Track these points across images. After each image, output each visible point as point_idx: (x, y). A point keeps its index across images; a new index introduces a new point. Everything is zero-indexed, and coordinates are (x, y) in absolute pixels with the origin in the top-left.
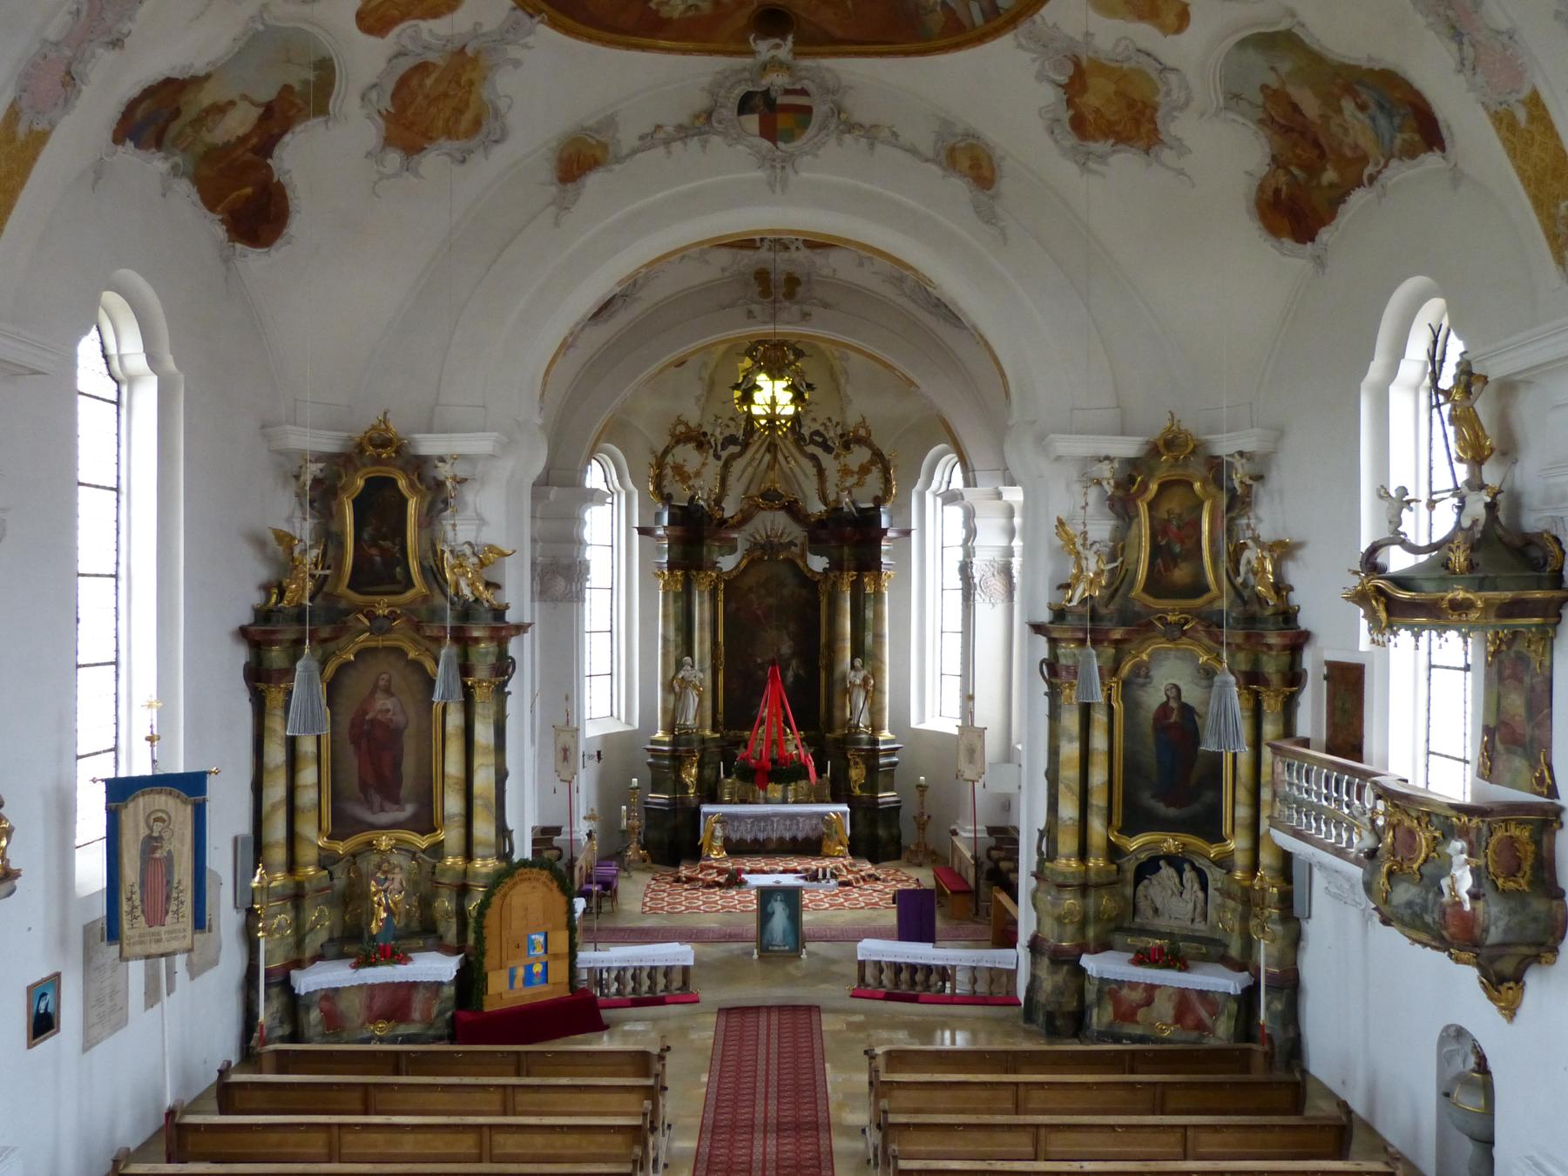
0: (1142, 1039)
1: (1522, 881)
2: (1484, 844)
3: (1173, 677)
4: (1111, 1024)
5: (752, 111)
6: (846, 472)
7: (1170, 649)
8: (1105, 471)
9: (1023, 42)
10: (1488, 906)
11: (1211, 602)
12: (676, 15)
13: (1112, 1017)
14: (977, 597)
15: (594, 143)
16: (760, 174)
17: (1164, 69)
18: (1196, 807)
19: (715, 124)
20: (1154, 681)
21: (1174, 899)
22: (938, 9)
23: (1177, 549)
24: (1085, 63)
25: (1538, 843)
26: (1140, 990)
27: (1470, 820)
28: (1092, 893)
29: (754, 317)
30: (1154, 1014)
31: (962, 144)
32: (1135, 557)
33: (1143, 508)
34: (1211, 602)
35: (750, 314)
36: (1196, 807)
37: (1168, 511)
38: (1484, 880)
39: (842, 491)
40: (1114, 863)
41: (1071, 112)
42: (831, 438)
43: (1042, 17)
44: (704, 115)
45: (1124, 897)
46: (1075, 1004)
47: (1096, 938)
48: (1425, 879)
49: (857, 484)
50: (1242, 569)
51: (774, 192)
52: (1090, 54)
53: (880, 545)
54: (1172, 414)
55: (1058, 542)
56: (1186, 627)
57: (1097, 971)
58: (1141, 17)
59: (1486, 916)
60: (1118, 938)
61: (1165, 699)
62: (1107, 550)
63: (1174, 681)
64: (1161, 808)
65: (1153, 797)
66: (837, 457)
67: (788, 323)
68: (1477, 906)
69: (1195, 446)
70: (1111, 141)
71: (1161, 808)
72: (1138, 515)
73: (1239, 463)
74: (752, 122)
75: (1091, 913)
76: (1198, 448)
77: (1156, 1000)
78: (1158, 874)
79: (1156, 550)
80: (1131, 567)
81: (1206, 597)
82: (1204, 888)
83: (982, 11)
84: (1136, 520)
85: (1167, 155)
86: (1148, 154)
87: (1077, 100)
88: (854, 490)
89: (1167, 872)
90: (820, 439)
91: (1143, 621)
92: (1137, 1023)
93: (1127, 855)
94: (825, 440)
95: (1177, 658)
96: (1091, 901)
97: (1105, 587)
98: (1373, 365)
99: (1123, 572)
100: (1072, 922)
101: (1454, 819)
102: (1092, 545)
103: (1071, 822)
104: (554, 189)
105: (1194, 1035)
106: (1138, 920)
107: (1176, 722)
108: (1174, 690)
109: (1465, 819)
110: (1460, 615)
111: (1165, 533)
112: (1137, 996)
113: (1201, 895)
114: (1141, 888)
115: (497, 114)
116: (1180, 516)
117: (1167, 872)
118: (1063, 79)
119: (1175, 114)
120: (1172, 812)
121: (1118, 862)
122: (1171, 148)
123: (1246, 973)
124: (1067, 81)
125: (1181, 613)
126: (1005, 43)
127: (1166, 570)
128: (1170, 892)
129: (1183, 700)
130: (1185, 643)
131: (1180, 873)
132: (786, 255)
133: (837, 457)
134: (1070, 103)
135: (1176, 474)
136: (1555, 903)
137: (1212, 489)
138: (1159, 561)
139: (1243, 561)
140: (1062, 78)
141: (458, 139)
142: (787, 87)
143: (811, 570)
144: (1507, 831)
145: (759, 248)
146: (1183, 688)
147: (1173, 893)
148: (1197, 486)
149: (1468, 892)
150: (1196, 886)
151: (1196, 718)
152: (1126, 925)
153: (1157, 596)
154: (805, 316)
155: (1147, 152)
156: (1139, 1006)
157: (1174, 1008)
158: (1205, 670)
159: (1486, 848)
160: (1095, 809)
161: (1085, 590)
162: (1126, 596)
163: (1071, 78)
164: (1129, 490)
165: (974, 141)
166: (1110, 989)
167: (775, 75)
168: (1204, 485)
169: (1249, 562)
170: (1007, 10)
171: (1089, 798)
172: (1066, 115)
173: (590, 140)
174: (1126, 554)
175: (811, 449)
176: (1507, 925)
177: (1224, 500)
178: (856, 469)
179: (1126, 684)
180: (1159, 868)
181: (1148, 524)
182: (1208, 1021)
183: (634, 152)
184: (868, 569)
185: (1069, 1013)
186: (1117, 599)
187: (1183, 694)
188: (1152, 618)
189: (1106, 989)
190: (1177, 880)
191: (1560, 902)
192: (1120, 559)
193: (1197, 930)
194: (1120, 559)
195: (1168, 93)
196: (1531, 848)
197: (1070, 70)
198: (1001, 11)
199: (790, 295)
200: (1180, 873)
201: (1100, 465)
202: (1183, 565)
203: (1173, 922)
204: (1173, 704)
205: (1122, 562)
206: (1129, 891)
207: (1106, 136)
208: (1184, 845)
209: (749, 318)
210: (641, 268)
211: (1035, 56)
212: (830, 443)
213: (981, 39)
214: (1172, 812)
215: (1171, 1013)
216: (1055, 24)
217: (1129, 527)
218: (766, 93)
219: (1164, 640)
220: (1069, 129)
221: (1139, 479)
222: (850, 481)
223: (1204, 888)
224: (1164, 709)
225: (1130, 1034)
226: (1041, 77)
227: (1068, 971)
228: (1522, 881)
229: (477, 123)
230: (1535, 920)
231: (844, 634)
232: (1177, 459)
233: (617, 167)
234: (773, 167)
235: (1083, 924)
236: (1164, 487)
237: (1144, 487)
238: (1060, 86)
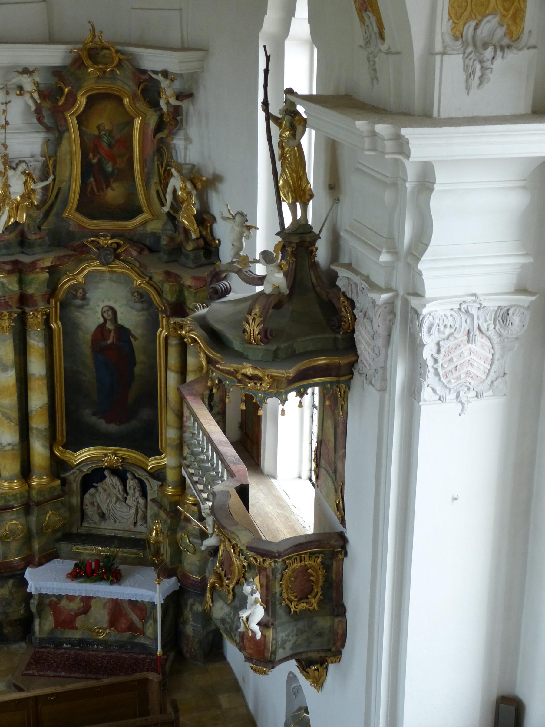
0: (82, 643)
1: (313, 601)
2: (279, 576)
3: (109, 300)
4: (52, 631)
7: (104, 272)
8: (28, 83)
10: (276, 632)
11: (145, 223)
13: (53, 625)
18: (134, 423)
20: (92, 303)
21: (118, 505)
23: (109, 168)
25: (327, 567)
26: (78, 600)
27: (264, 561)
28: (35, 511)
30: (92, 620)
32: (67, 174)
33: (72, 122)
36: (134, 423)
37: (98, 127)
38: (278, 607)
40: (58, 477)
45: (71, 508)
46: (22, 612)
47: (42, 550)
48: (236, 599)
50: (169, 198)
57: (36, 589)
59: (274, 642)
60: (64, 547)
61: (101, 321)
62: (39, 165)
64: (102, 424)
65: (94, 414)
68: (267, 634)
71: (102, 424)
72: (68, 130)
73: (164, 83)
75: (34, 529)
77: (92, 608)
78: (104, 481)
80: (64, 185)
81: (139, 219)
82: (144, 494)
84: (66, 134)
89: (111, 480)
91: (76, 243)
92: (76, 628)
93: (72, 468)
95: (111, 280)
96: (33, 519)
97: (38, 207)
98: (266, 17)
100: (15, 539)
101: (251, 559)
102: (17, 165)
103: (9, 447)
105: (127, 635)
106: (85, 524)
107: (111, 344)
108: (110, 312)
109: (260, 559)
110: (255, 384)
111: (96, 150)
112: (74, 606)
113: (141, 501)
114: (87, 496)
116: (111, 132)
117: (111, 480)
120: (112, 428)
121: (63, 476)
123: (174, 579)
125: (112, 238)
127: (98, 191)
128: (114, 498)
130: (119, 267)
131: (124, 481)
135: (104, 87)
136: (336, 620)
137: (141, 106)
138: (92, 179)
139: (170, 189)
144: (301, 561)
146: (119, 311)
147: (118, 499)
148: (126, 101)
149: (259, 624)
150: (137, 494)
151: (132, 340)
152: (74, 530)
153: (91, 217)
156: (77, 614)
157: (109, 614)
158: (139, 293)
159: (281, 580)
161: (10, 217)
162: (59, 215)
164: (58, 101)
166: (50, 601)
169: (175, 191)
171: (30, 422)
174: (57, 173)
176: (295, 643)
177: (153, 121)
179: (64, 305)
180: (105, 477)
181: (79, 141)
182: (139, 625)
185: (16, 621)
186: (51, 218)
187: (119, 316)
189: (47, 601)
190: (121, 488)
191: (340, 619)
192: (52, 177)
193: (140, 533)
194: (52, 177)
196: (321, 572)
200: (124, 481)
202: (115, 185)
203: (117, 526)
205: (54, 180)
206: (75, 500)
208: (123, 459)
214: (112, 428)
215: (107, 618)
217: (58, 142)
219: (98, 263)
221: (66, 90)
223: (144, 494)
224: (102, 327)
225: (70, 639)
227: (13, 584)
228: (313, 601)
230: (320, 635)
235: (28, 538)
236: (92, 100)
237: (72, 99)
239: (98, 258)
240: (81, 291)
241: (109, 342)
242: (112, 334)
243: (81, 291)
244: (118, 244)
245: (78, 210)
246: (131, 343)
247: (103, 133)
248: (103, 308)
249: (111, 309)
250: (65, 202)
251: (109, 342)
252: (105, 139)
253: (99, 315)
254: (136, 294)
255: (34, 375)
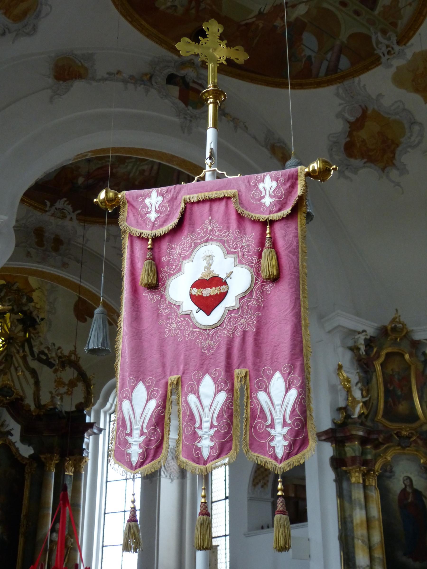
5: (175, 84)
6: (59, 383)
9: (341, 91)
12: (162, 8)
14: (162, 473)
15: (80, 64)
16: (176, 120)
17: (413, 123)
19: (154, 83)
22: (304, 60)
23: (399, 392)
24: (369, 112)
29: (31, 257)
31: (278, 145)
34: (421, 426)
35: (28, 254)
37: (392, 370)
39: (58, 395)
41: (348, 139)
42: (52, 357)
43: (360, 81)
44: (148, 76)
49: (66, 393)
51: (184, 132)
52: (376, 107)
53: (83, 438)
54: (397, 310)
55: (335, 380)
56: (412, 439)
58: (417, 91)
61: (403, 486)
63: (409, 475)
66: (55, 371)
67: (53, 266)
69: (407, 333)
70: (365, 160)
74: (175, 90)
76: (407, 336)
79: (387, 392)
80: (375, 402)
83: (328, 67)
84: (374, 374)
85: (394, 173)
86: (383, 171)
87: (355, 133)
88: (65, 396)
90: (44, 358)
94: (48, 358)
99: (371, 404)
104: (51, 81)
108: (408, 480)
115: (38, 16)
118: (352, 119)
119: (409, 149)
122: (398, 169)
124: (354, 121)
126: (329, 90)
129: (415, 487)
132: (60, 222)
133: (55, 371)
134: (350, 134)
135: (394, 349)
138: (390, 399)
140: (352, 118)
141: (9, 18)
142: (194, 79)
143: (20, 455)
145: (47, 211)
146: (414, 479)
148: (407, 356)
151: (424, 499)
153: (391, 420)
154: (64, 265)
155: (383, 170)
160: (377, 560)
163: (357, 120)
165: (284, 146)
167: (191, 69)
168: (411, 355)
170: (342, 71)
172: (343, 141)
173: (77, 62)
175: (34, 364)
178: (67, 382)
183: (104, 79)
184: (72, 454)
187: (414, 483)
188: (393, 433)
195: (410, 138)
197: (359, 114)
198: (339, 71)
199: (56, 249)
201: (360, 335)
204: (409, 490)
205: (370, 398)
207: (363, 158)
209: (27, 256)
210: (89, 152)
211: (342, 102)
212: (52, 360)
213: (319, 85)
216: (365, 85)
218: (183, 78)
220: (342, 148)
222: (63, 390)
224: (404, 491)
226: (339, 115)
229: (25, 14)
231: (49, 503)
232: (396, 339)
233: (94, 84)
234: (185, 118)
236: (388, 355)
238: (349, 122)
239: (399, 445)
240: (389, 467)
241: (410, 501)
242: (411, 496)
243: (389, 467)
244: (412, 434)
245: (383, 416)
246: (422, 501)
247: (395, 373)
248: (404, 477)
249: (409, 478)
250: (376, 413)
251: (410, 501)
252: (396, 377)
253: (401, 482)
254: (423, 468)
255: (374, 517)
